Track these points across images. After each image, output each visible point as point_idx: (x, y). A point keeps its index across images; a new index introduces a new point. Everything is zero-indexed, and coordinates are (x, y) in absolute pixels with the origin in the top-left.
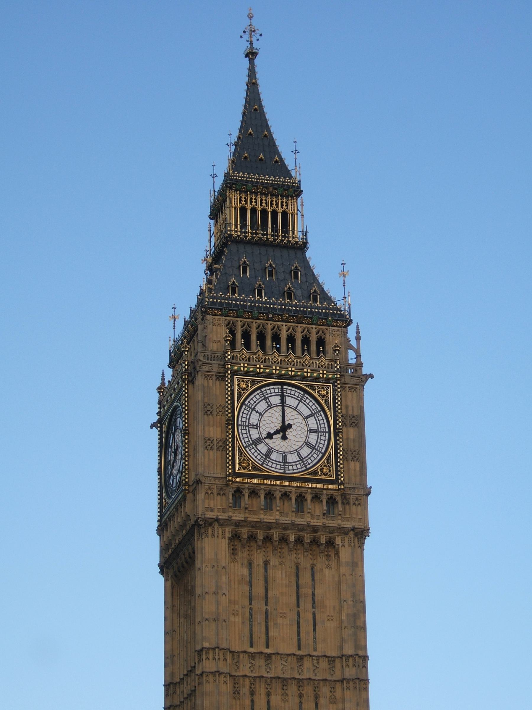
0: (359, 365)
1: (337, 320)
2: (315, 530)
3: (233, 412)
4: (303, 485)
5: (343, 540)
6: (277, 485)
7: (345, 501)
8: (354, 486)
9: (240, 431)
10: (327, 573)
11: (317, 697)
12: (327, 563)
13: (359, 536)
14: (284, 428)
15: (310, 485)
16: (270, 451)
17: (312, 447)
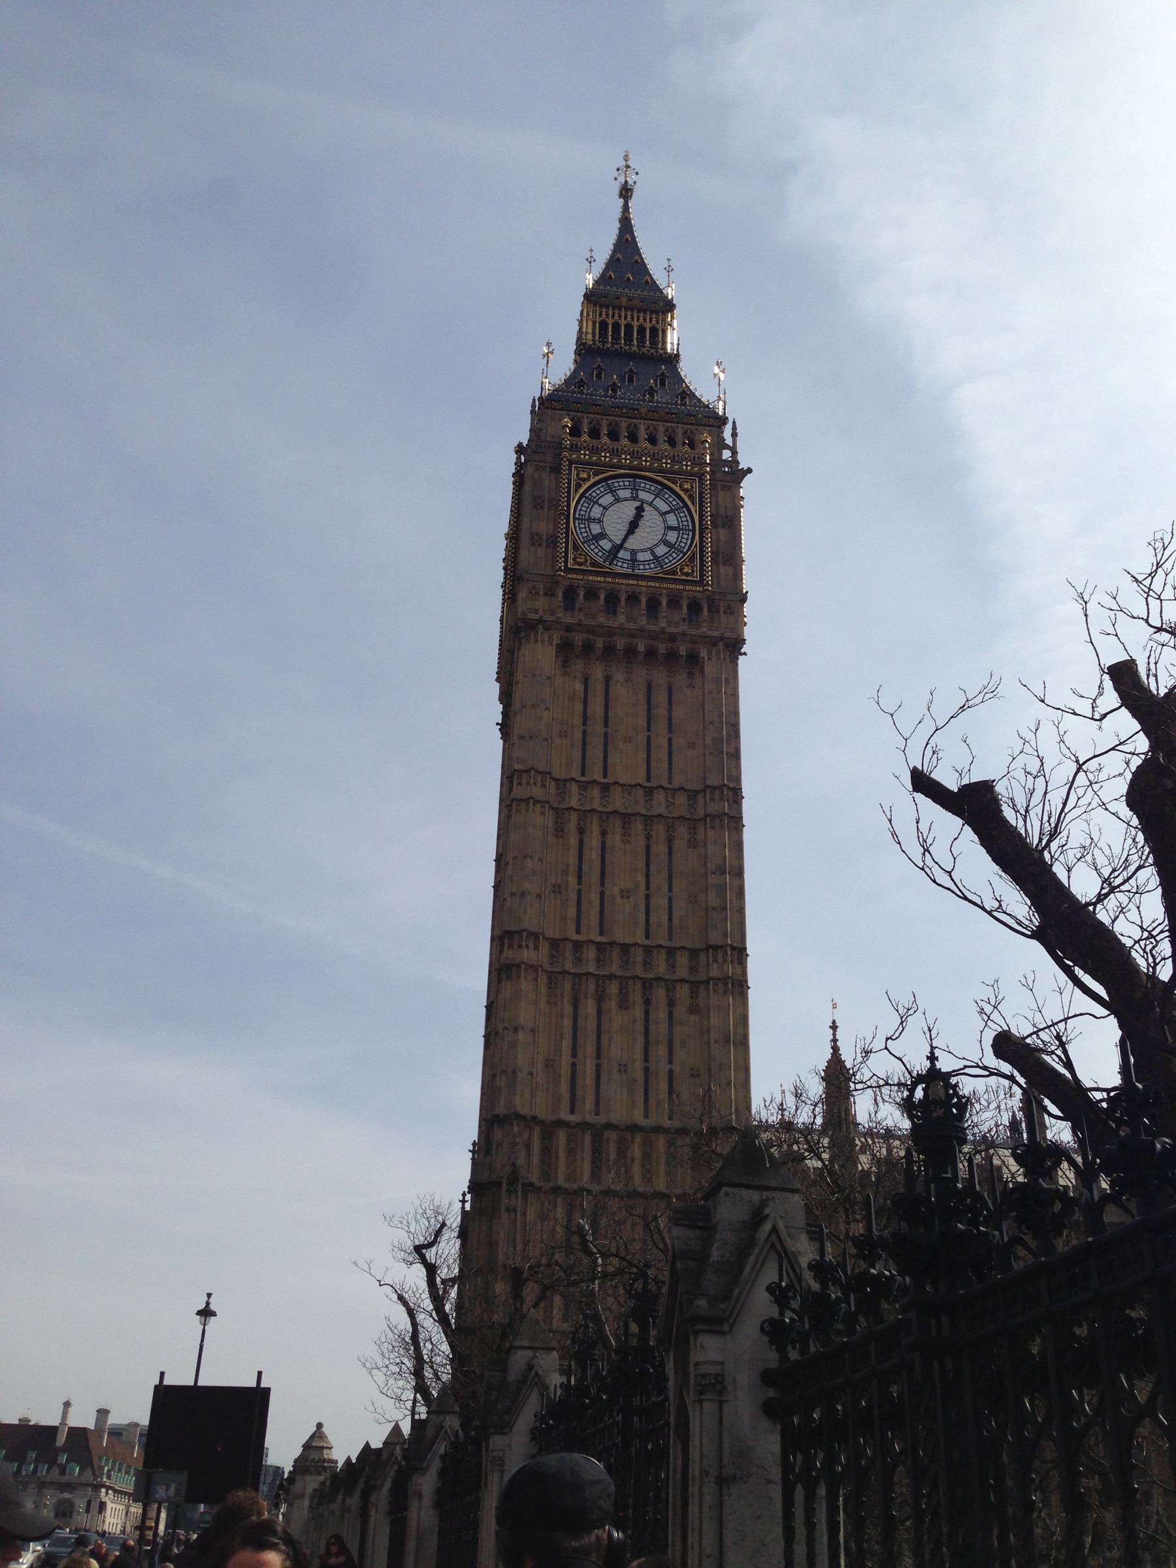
0: (735, 461)
2: (672, 638)
5: (710, 653)
11: (670, 841)
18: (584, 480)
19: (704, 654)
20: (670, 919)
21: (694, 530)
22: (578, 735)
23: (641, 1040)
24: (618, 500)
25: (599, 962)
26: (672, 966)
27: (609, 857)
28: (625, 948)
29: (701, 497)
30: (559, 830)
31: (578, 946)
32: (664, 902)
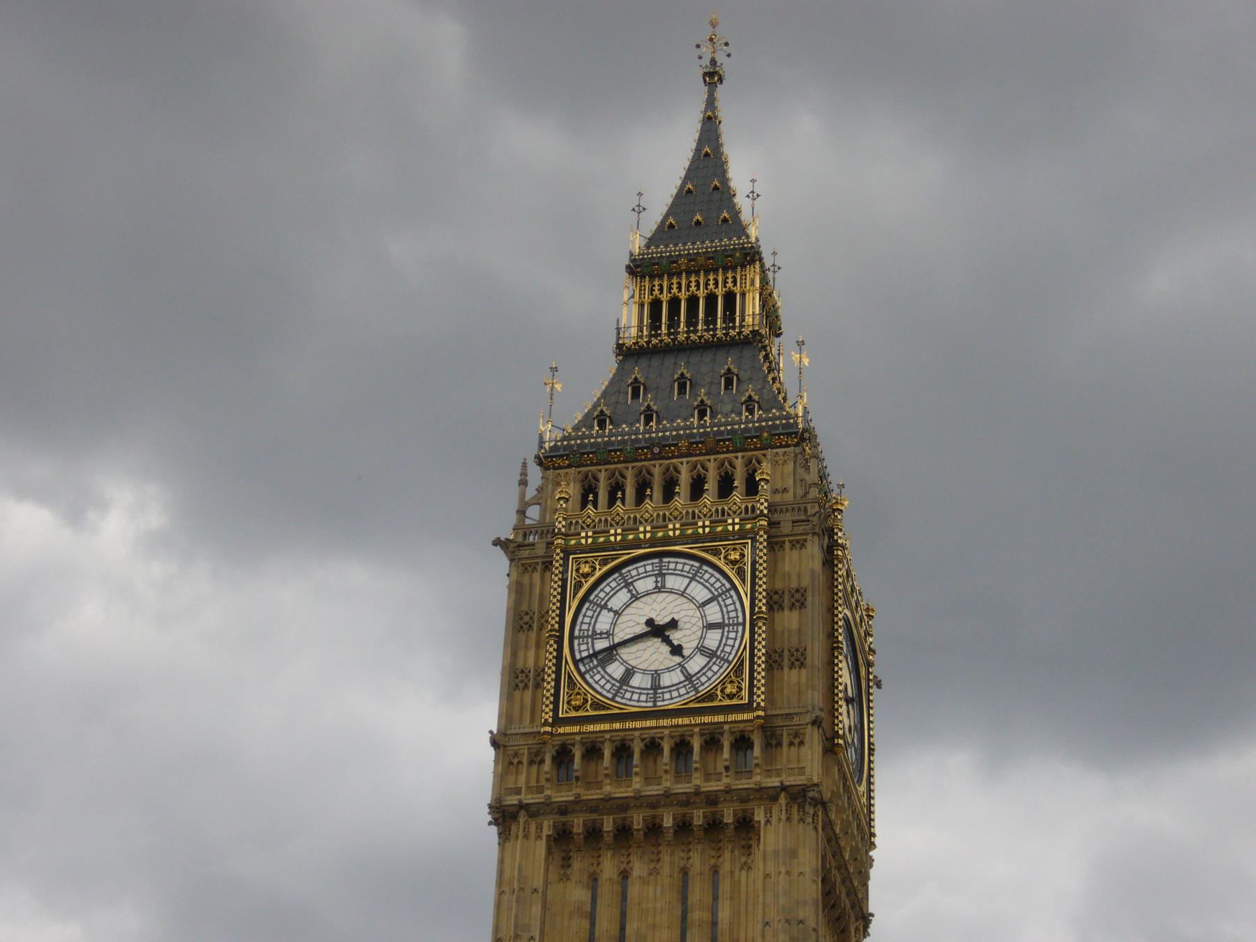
1: (779, 435)
2: (712, 800)
3: (562, 616)
4: (686, 721)
5: (769, 812)
6: (635, 729)
7: (774, 742)
8: (792, 711)
9: (576, 647)
10: (743, 878)
12: (743, 859)
13: (800, 800)
14: (657, 631)
15: (698, 720)
16: (629, 673)
17: (712, 655)
18: (586, 576)
19: (759, 816)
21: (744, 624)
24: (635, 597)
29: (754, 570)
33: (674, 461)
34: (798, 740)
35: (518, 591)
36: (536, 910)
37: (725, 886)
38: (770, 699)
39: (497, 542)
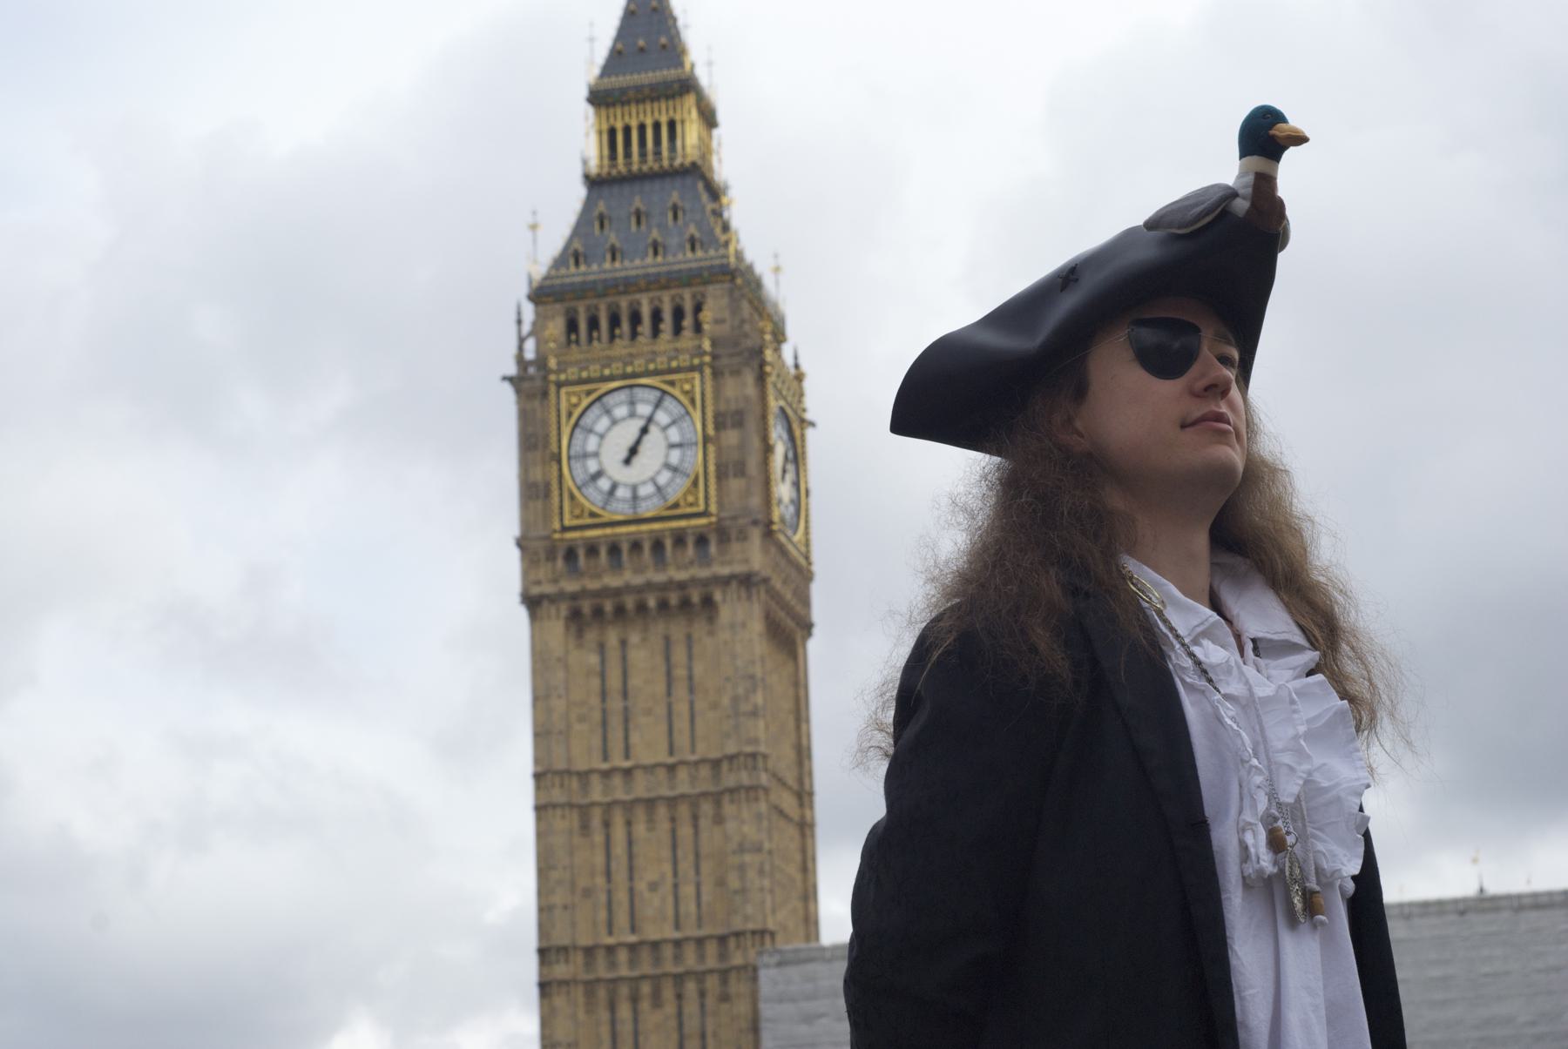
2: (682, 586)
3: (559, 441)
5: (724, 593)
11: (695, 818)
16: (614, 486)
17: (675, 470)
18: (576, 406)
19: (718, 596)
20: (699, 905)
22: (597, 716)
23: (675, 1036)
24: (614, 422)
25: (633, 963)
26: (701, 958)
27: (636, 849)
28: (655, 945)
29: (703, 401)
30: (585, 828)
31: (610, 950)
32: (688, 890)
33: (637, 296)
34: (743, 537)
35: (525, 417)
36: (560, 675)
37: (696, 650)
38: (720, 504)
39: (505, 378)
